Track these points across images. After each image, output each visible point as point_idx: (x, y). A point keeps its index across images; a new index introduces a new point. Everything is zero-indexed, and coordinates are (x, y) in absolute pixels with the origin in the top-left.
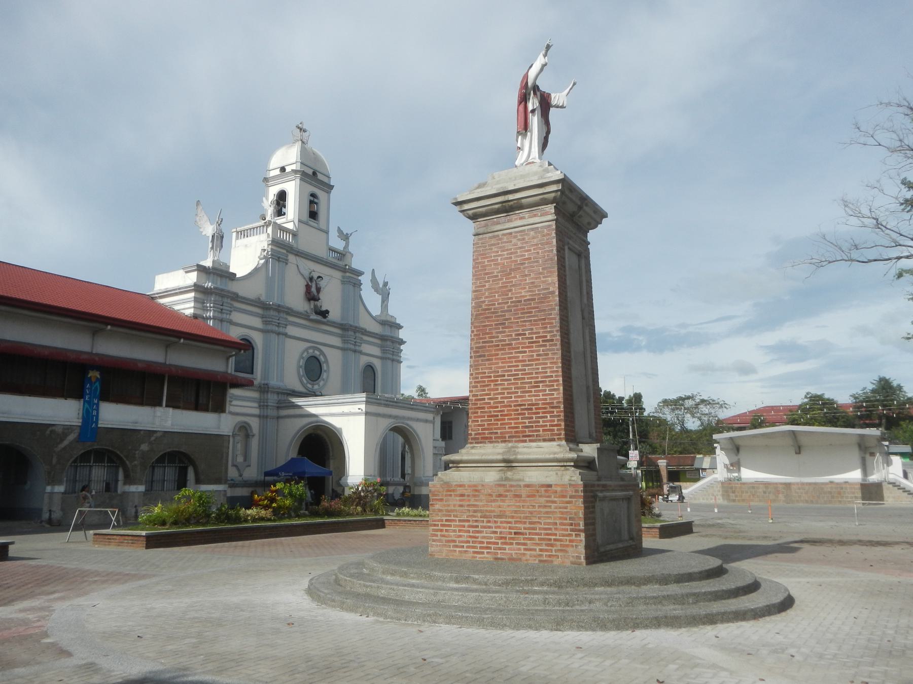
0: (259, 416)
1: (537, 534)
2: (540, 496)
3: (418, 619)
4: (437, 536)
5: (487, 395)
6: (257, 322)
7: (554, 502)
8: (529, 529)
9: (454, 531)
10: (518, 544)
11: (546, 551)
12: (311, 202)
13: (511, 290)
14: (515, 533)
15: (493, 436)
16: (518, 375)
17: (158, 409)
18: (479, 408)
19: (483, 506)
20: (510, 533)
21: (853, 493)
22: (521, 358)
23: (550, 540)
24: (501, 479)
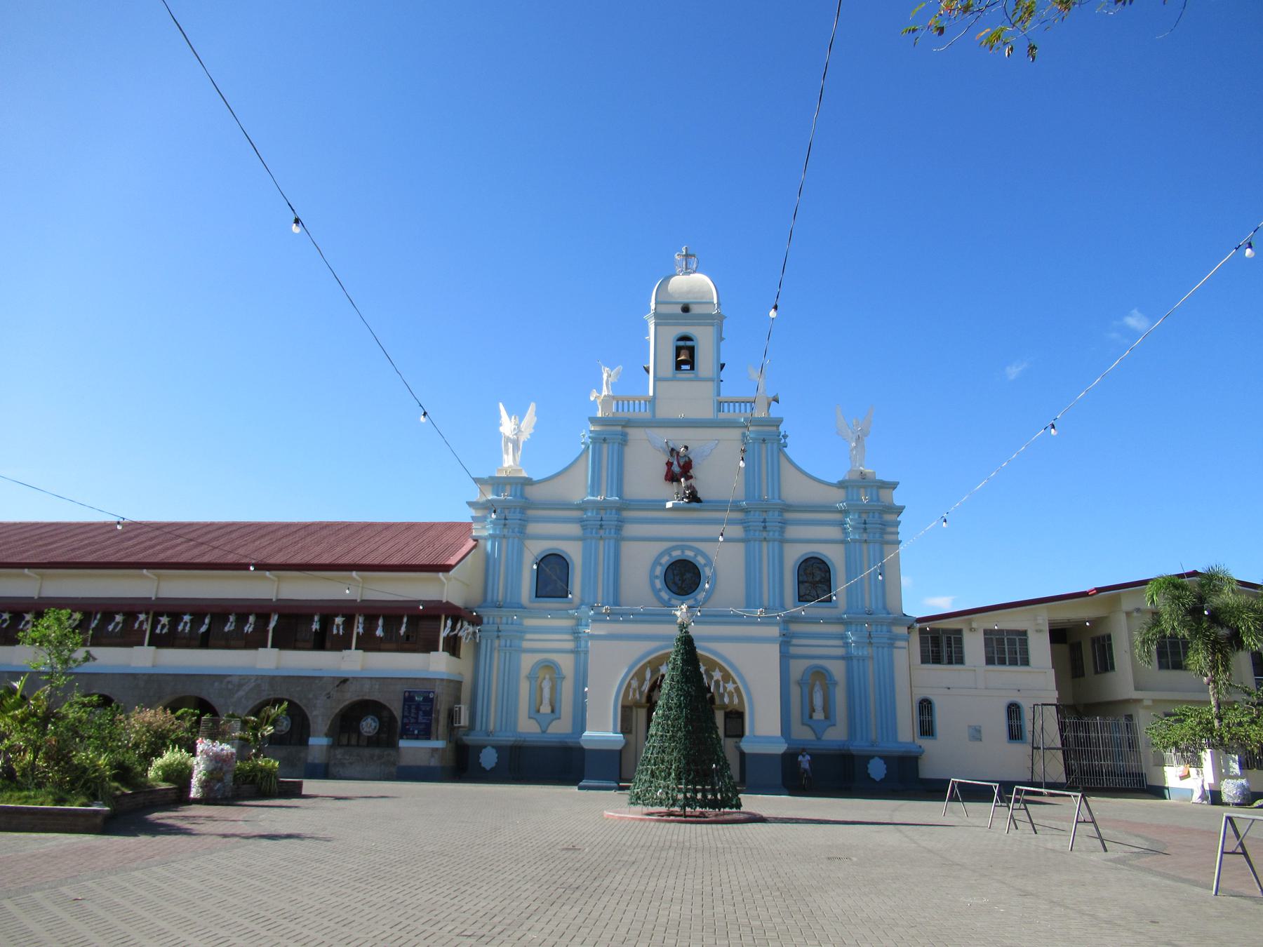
0: (572, 652)
6: (575, 529)
12: (678, 350)
17: (346, 653)
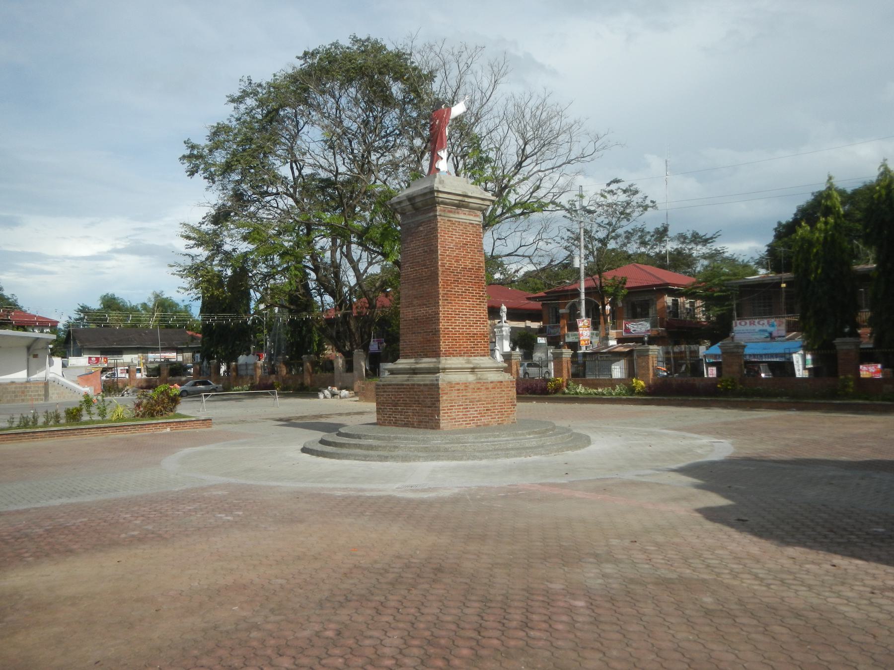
1: (496, 409)
2: (498, 388)
3: (556, 452)
4: (445, 416)
5: (450, 325)
7: (504, 391)
8: (493, 407)
9: (455, 412)
10: (488, 416)
11: (501, 418)
13: (461, 260)
14: (487, 410)
15: (455, 352)
16: (466, 315)
18: (446, 334)
19: (470, 395)
20: (484, 410)
21: (37, 391)
22: (468, 305)
23: (502, 412)
24: (477, 379)
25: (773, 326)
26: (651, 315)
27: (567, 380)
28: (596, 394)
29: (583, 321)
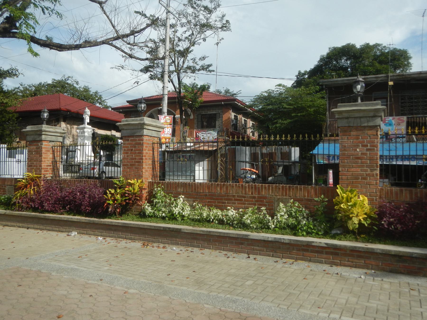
25: (390, 125)
26: (217, 126)
27: (151, 184)
28: (221, 222)
29: (165, 117)
